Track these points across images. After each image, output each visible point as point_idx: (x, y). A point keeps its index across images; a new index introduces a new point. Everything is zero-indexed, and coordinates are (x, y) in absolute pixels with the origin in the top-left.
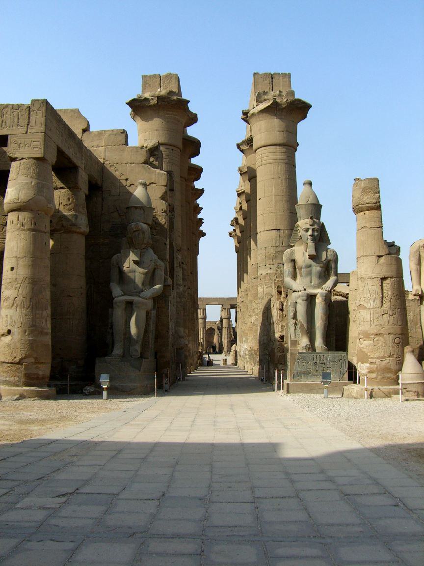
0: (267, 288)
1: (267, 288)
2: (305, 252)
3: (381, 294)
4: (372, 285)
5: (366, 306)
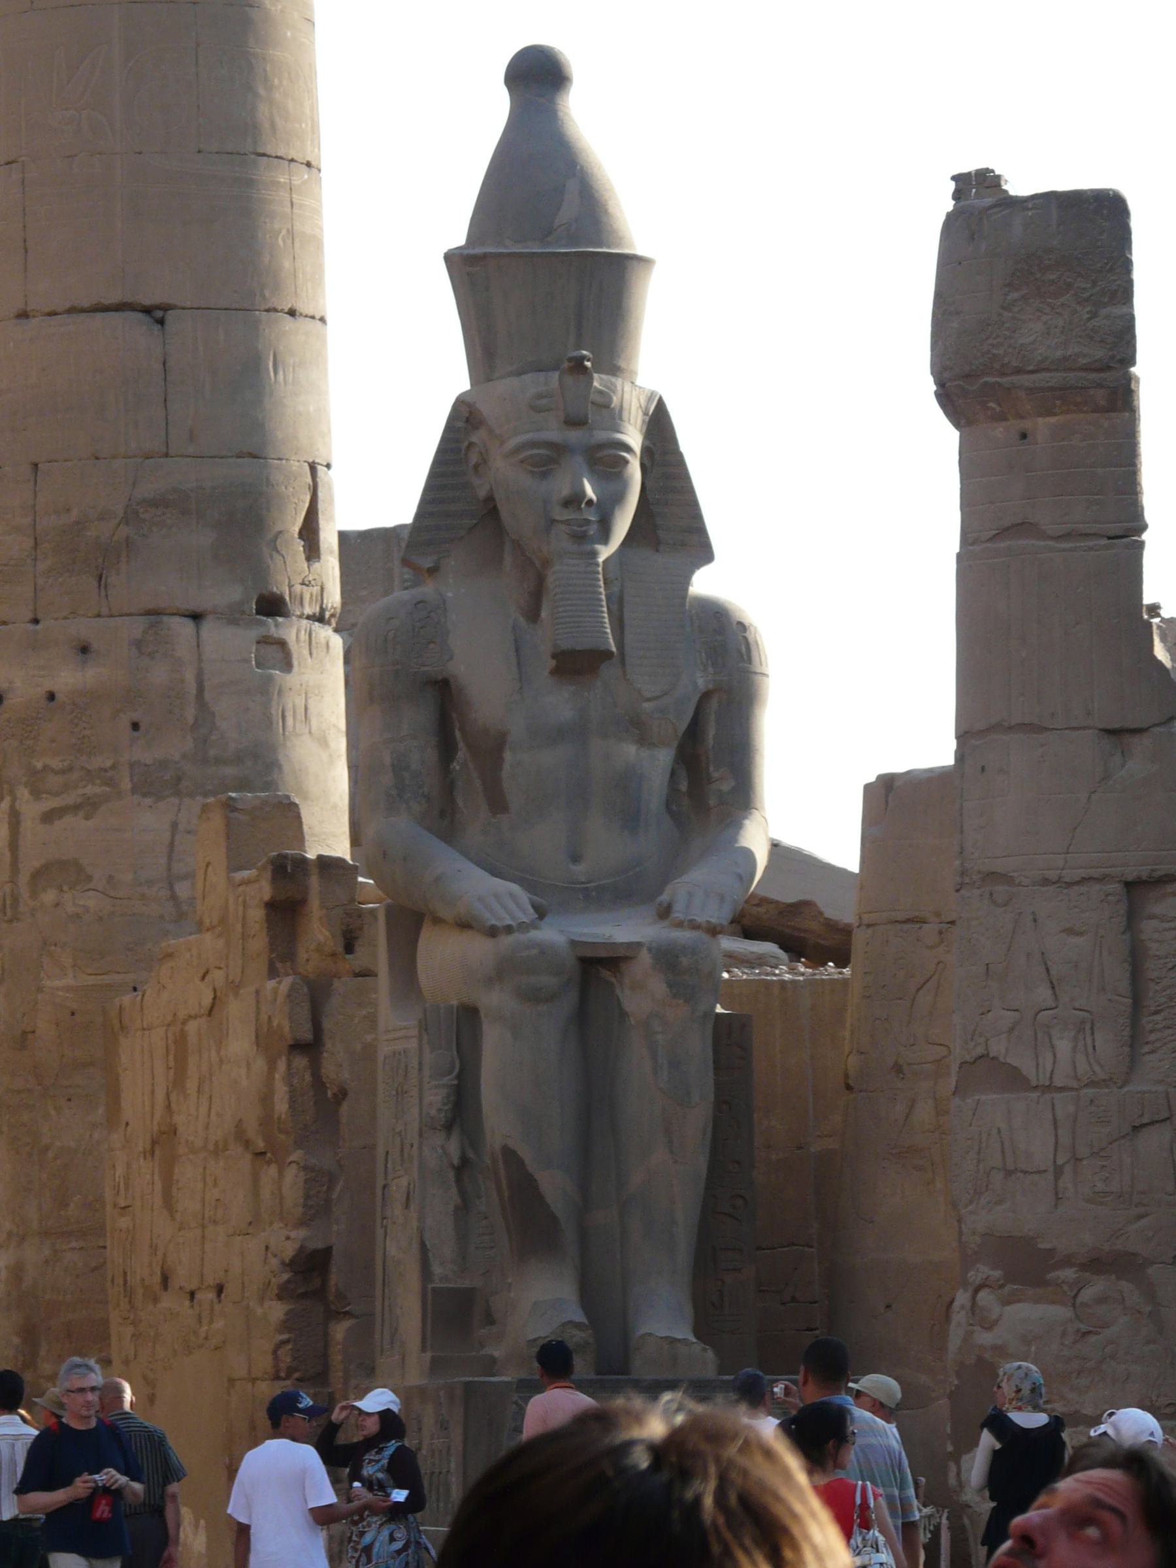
0: (48, 817)
1: (48, 817)
2: (522, 620)
3: (1124, 986)
4: (1070, 931)
5: (1026, 1066)
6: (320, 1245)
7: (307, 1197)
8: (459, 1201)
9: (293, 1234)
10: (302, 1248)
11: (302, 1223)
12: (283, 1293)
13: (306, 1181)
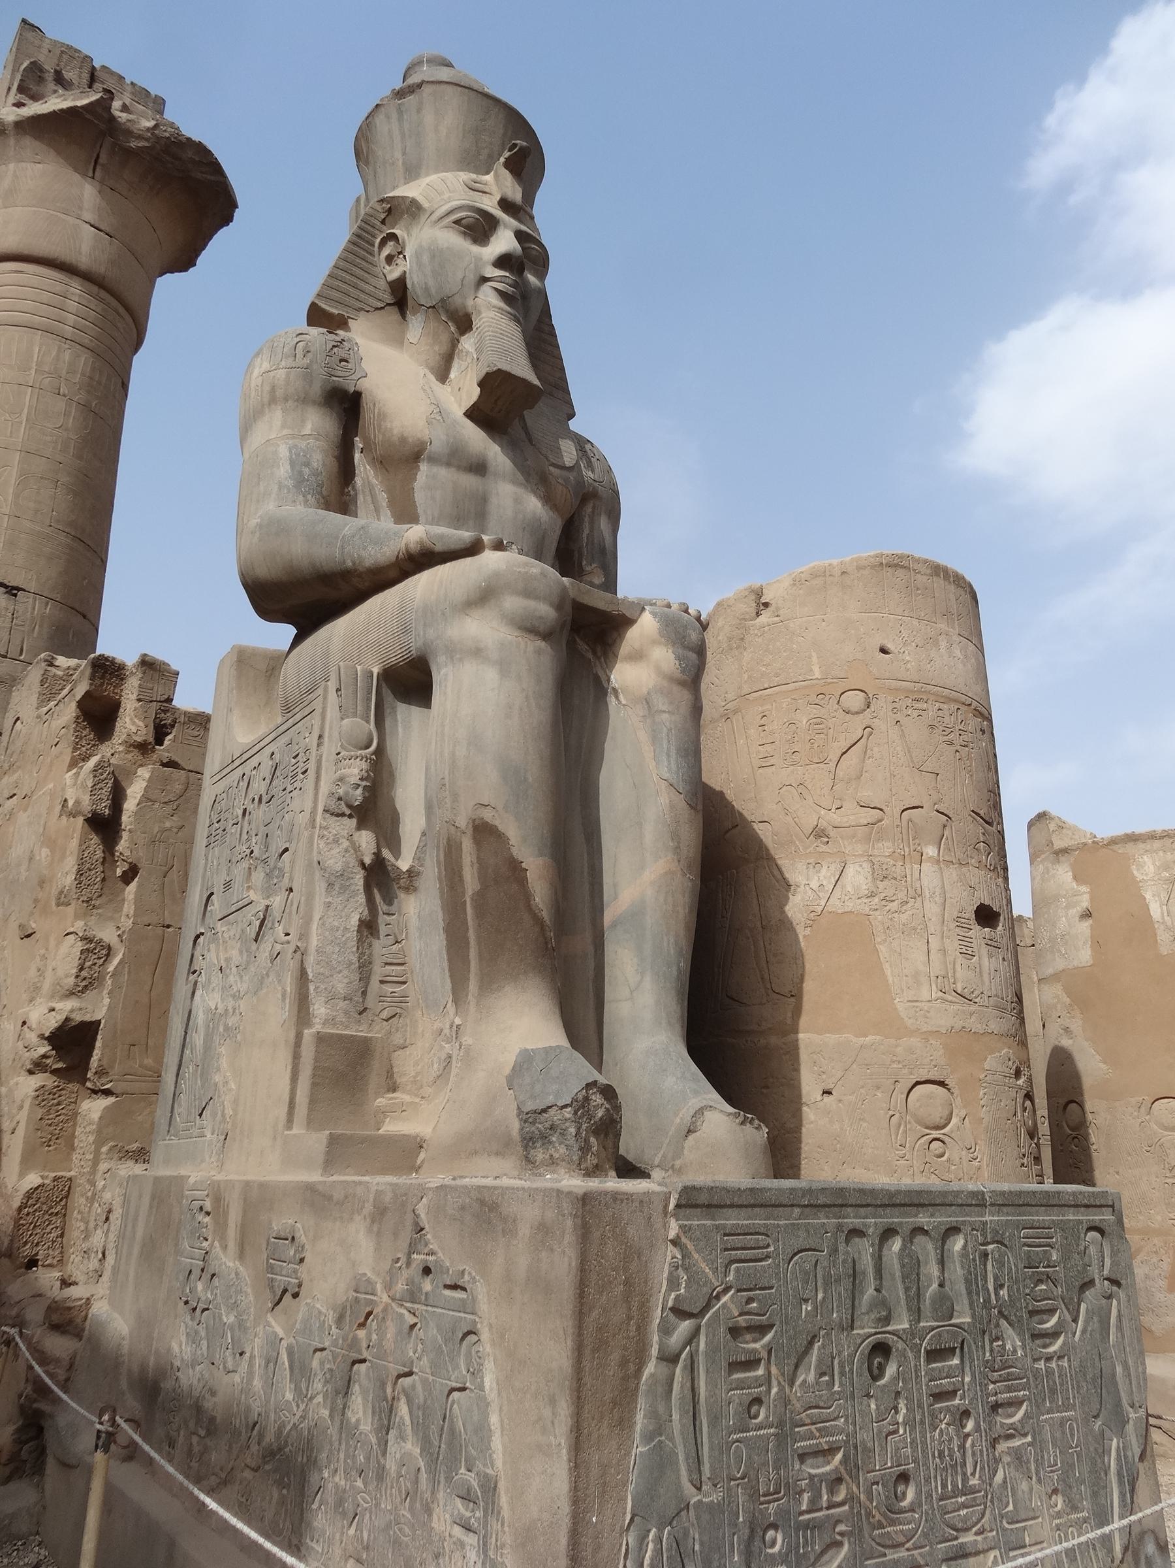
6: (88, 1018)
7: (81, 969)
8: (366, 912)
9: (58, 1005)
10: (67, 1019)
11: (71, 994)
12: (38, 1066)
13: (82, 952)
